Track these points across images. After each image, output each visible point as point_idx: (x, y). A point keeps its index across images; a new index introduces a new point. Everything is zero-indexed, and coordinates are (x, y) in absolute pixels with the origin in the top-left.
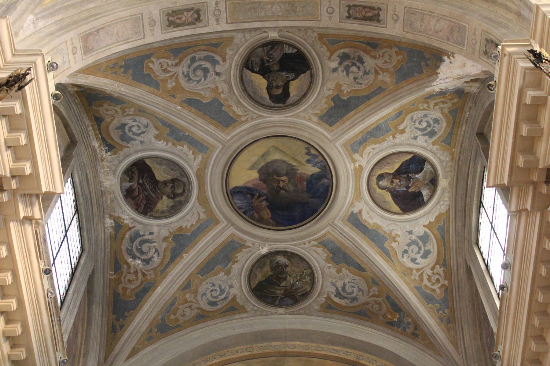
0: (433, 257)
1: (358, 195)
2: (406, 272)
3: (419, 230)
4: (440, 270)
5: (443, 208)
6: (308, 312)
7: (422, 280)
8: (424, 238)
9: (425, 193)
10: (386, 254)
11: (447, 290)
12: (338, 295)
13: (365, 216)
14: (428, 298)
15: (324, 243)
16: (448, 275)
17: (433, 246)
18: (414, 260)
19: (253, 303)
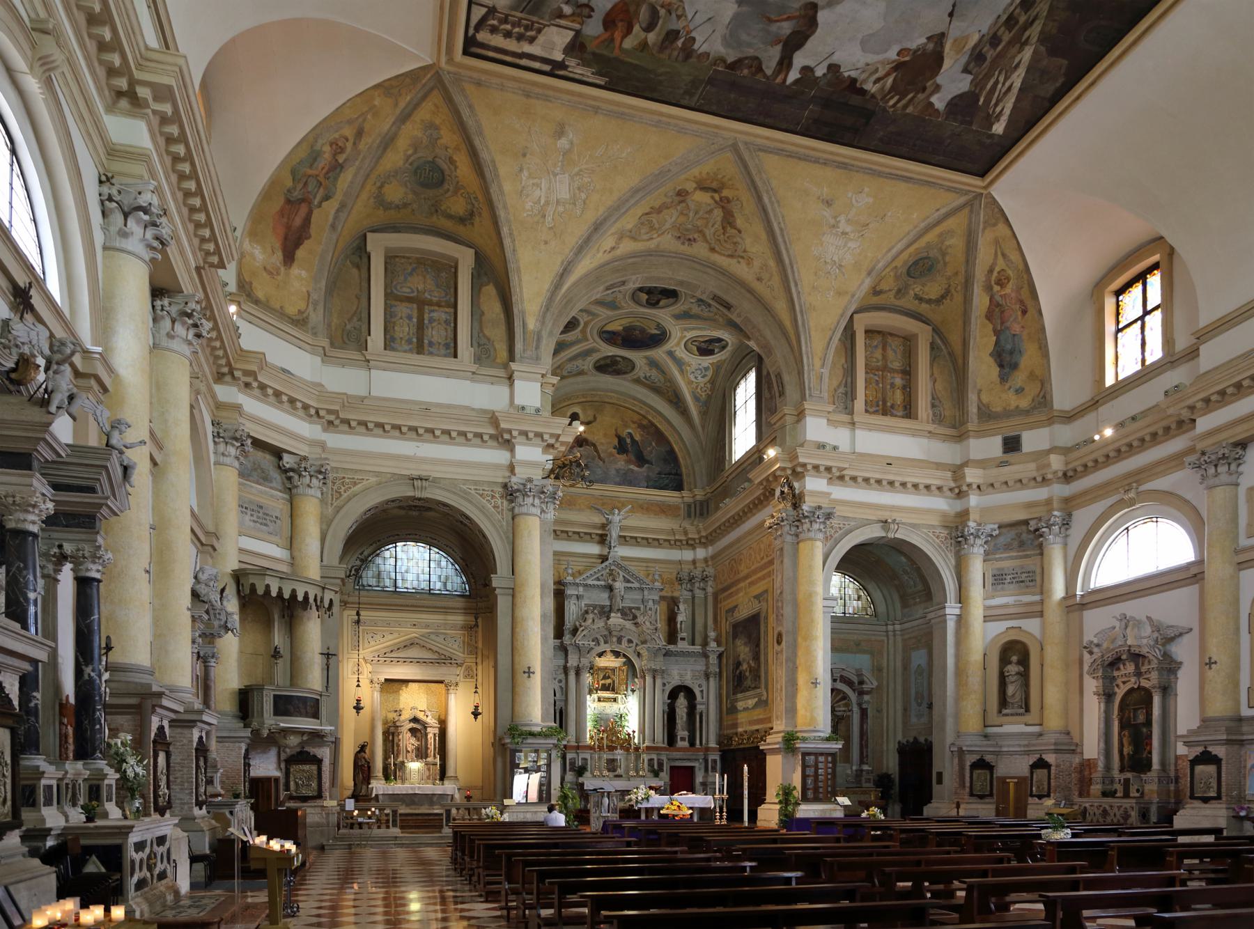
0: (707, 379)
1: (678, 344)
2: (690, 383)
3: (706, 364)
4: (709, 385)
5: (723, 358)
6: (625, 379)
7: (697, 387)
8: (706, 369)
9: (716, 351)
10: (682, 371)
11: (709, 397)
12: (645, 378)
13: (677, 353)
14: (696, 398)
15: (646, 358)
16: (712, 389)
17: (710, 373)
18: (696, 378)
19: (594, 372)
